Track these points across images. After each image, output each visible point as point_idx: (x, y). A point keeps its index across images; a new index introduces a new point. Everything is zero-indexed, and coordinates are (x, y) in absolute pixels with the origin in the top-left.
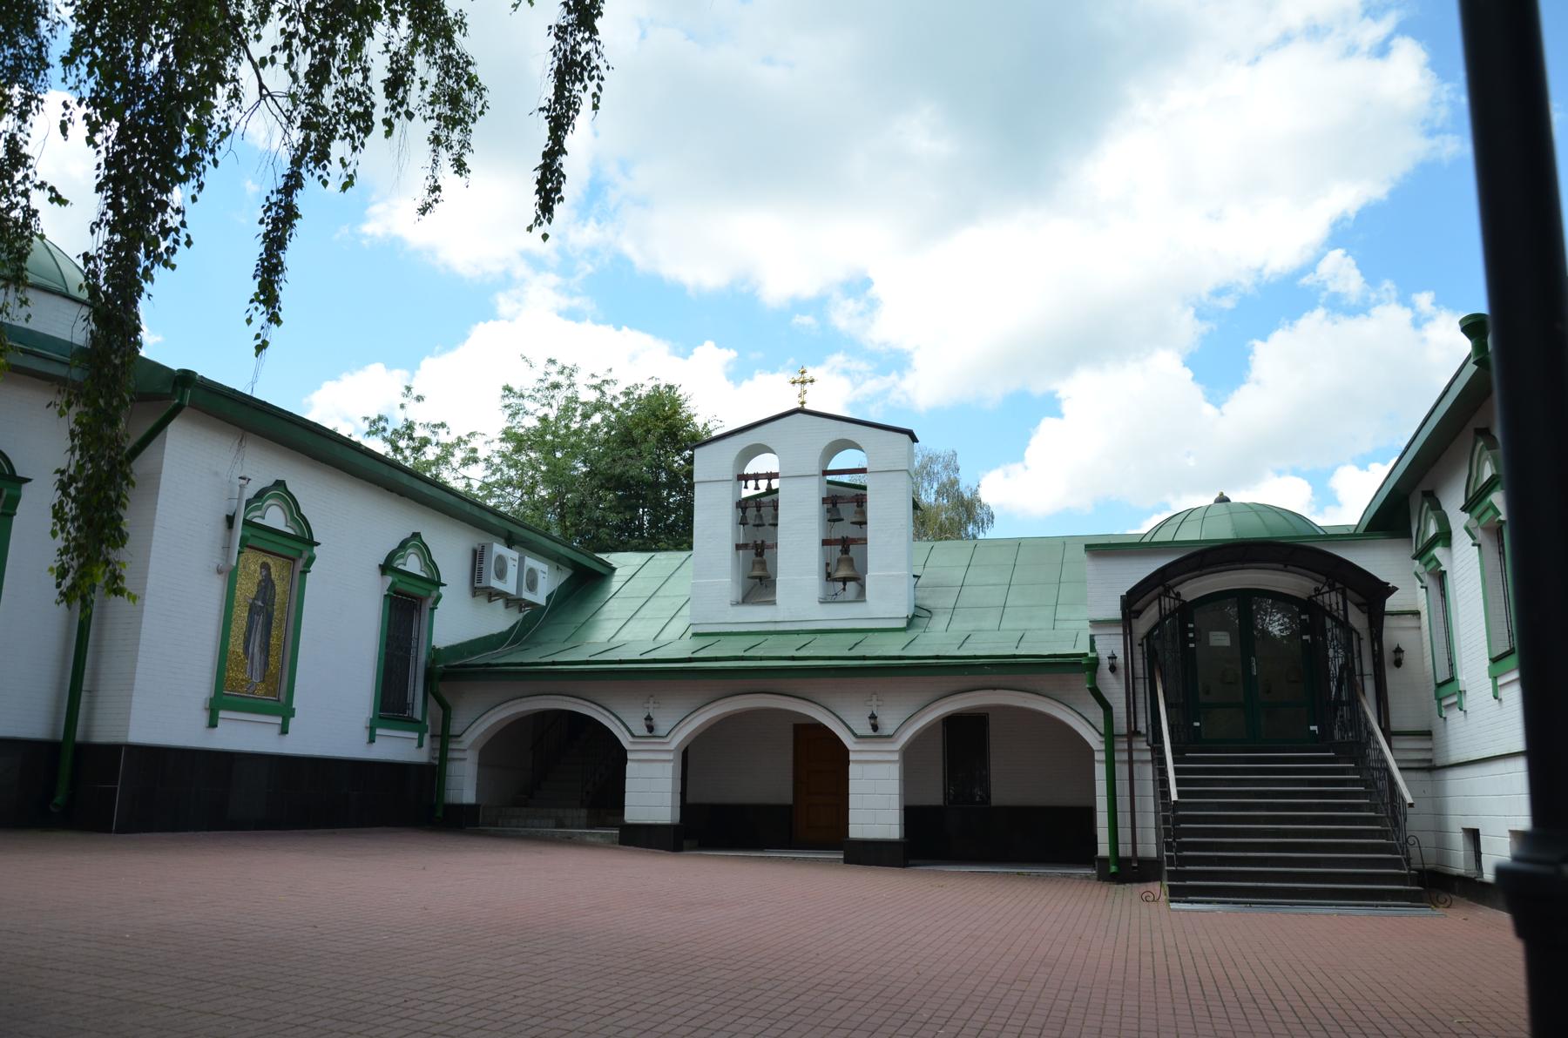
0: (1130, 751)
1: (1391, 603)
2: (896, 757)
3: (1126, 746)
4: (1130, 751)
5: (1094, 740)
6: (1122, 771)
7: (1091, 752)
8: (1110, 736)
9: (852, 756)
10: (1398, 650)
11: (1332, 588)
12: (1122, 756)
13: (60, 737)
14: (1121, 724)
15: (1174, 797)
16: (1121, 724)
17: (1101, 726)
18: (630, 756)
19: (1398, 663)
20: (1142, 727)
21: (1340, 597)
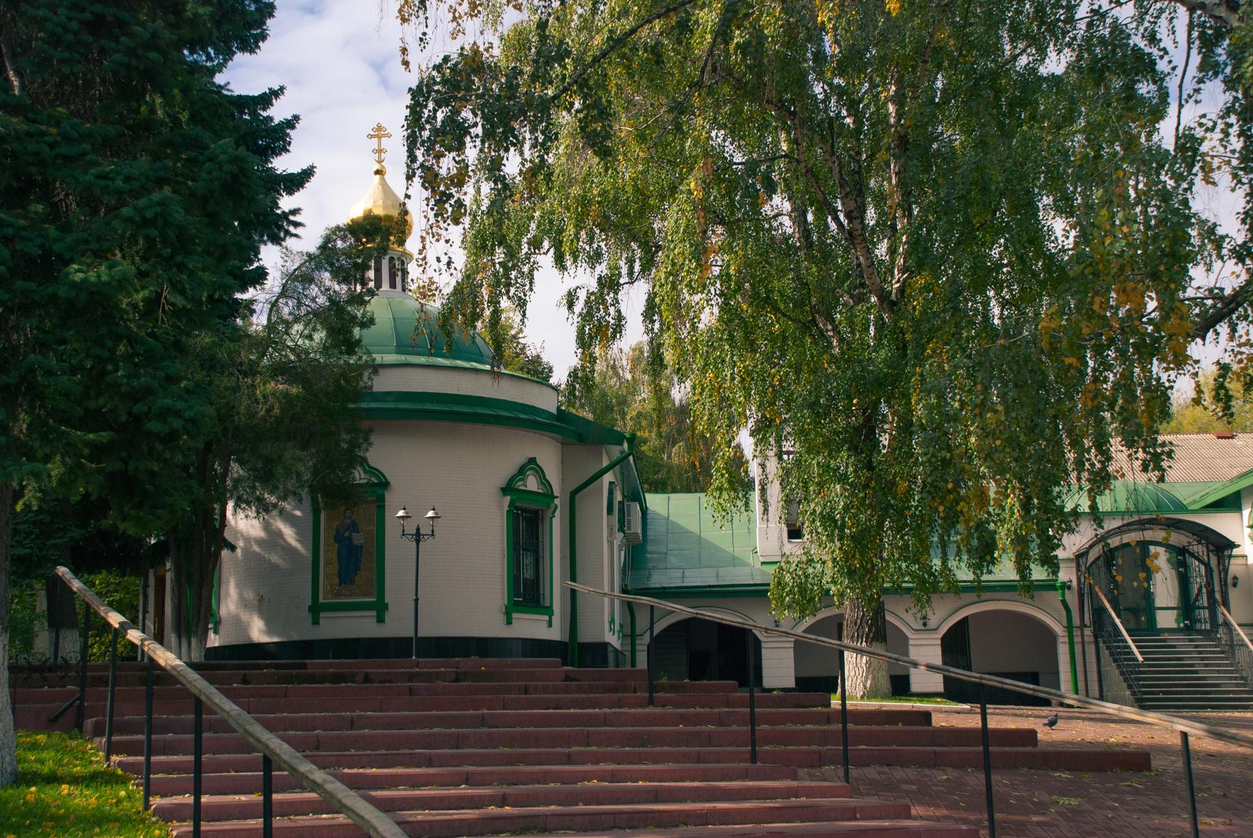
0: (1083, 636)
1: (1235, 551)
2: (939, 642)
3: (1079, 633)
4: (1083, 636)
5: (1058, 629)
6: (1078, 648)
7: (1051, 636)
8: (1069, 628)
9: (911, 642)
10: (1235, 578)
11: (1199, 542)
12: (1077, 639)
13: (567, 640)
14: (1076, 621)
15: (1140, 658)
16: (1076, 621)
17: (1065, 622)
18: (763, 645)
19: (1235, 585)
20: (1087, 621)
21: (1205, 549)
